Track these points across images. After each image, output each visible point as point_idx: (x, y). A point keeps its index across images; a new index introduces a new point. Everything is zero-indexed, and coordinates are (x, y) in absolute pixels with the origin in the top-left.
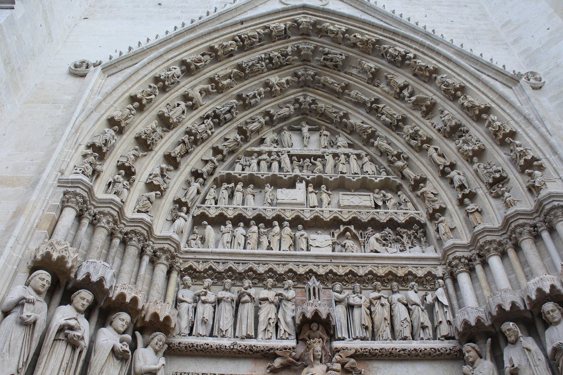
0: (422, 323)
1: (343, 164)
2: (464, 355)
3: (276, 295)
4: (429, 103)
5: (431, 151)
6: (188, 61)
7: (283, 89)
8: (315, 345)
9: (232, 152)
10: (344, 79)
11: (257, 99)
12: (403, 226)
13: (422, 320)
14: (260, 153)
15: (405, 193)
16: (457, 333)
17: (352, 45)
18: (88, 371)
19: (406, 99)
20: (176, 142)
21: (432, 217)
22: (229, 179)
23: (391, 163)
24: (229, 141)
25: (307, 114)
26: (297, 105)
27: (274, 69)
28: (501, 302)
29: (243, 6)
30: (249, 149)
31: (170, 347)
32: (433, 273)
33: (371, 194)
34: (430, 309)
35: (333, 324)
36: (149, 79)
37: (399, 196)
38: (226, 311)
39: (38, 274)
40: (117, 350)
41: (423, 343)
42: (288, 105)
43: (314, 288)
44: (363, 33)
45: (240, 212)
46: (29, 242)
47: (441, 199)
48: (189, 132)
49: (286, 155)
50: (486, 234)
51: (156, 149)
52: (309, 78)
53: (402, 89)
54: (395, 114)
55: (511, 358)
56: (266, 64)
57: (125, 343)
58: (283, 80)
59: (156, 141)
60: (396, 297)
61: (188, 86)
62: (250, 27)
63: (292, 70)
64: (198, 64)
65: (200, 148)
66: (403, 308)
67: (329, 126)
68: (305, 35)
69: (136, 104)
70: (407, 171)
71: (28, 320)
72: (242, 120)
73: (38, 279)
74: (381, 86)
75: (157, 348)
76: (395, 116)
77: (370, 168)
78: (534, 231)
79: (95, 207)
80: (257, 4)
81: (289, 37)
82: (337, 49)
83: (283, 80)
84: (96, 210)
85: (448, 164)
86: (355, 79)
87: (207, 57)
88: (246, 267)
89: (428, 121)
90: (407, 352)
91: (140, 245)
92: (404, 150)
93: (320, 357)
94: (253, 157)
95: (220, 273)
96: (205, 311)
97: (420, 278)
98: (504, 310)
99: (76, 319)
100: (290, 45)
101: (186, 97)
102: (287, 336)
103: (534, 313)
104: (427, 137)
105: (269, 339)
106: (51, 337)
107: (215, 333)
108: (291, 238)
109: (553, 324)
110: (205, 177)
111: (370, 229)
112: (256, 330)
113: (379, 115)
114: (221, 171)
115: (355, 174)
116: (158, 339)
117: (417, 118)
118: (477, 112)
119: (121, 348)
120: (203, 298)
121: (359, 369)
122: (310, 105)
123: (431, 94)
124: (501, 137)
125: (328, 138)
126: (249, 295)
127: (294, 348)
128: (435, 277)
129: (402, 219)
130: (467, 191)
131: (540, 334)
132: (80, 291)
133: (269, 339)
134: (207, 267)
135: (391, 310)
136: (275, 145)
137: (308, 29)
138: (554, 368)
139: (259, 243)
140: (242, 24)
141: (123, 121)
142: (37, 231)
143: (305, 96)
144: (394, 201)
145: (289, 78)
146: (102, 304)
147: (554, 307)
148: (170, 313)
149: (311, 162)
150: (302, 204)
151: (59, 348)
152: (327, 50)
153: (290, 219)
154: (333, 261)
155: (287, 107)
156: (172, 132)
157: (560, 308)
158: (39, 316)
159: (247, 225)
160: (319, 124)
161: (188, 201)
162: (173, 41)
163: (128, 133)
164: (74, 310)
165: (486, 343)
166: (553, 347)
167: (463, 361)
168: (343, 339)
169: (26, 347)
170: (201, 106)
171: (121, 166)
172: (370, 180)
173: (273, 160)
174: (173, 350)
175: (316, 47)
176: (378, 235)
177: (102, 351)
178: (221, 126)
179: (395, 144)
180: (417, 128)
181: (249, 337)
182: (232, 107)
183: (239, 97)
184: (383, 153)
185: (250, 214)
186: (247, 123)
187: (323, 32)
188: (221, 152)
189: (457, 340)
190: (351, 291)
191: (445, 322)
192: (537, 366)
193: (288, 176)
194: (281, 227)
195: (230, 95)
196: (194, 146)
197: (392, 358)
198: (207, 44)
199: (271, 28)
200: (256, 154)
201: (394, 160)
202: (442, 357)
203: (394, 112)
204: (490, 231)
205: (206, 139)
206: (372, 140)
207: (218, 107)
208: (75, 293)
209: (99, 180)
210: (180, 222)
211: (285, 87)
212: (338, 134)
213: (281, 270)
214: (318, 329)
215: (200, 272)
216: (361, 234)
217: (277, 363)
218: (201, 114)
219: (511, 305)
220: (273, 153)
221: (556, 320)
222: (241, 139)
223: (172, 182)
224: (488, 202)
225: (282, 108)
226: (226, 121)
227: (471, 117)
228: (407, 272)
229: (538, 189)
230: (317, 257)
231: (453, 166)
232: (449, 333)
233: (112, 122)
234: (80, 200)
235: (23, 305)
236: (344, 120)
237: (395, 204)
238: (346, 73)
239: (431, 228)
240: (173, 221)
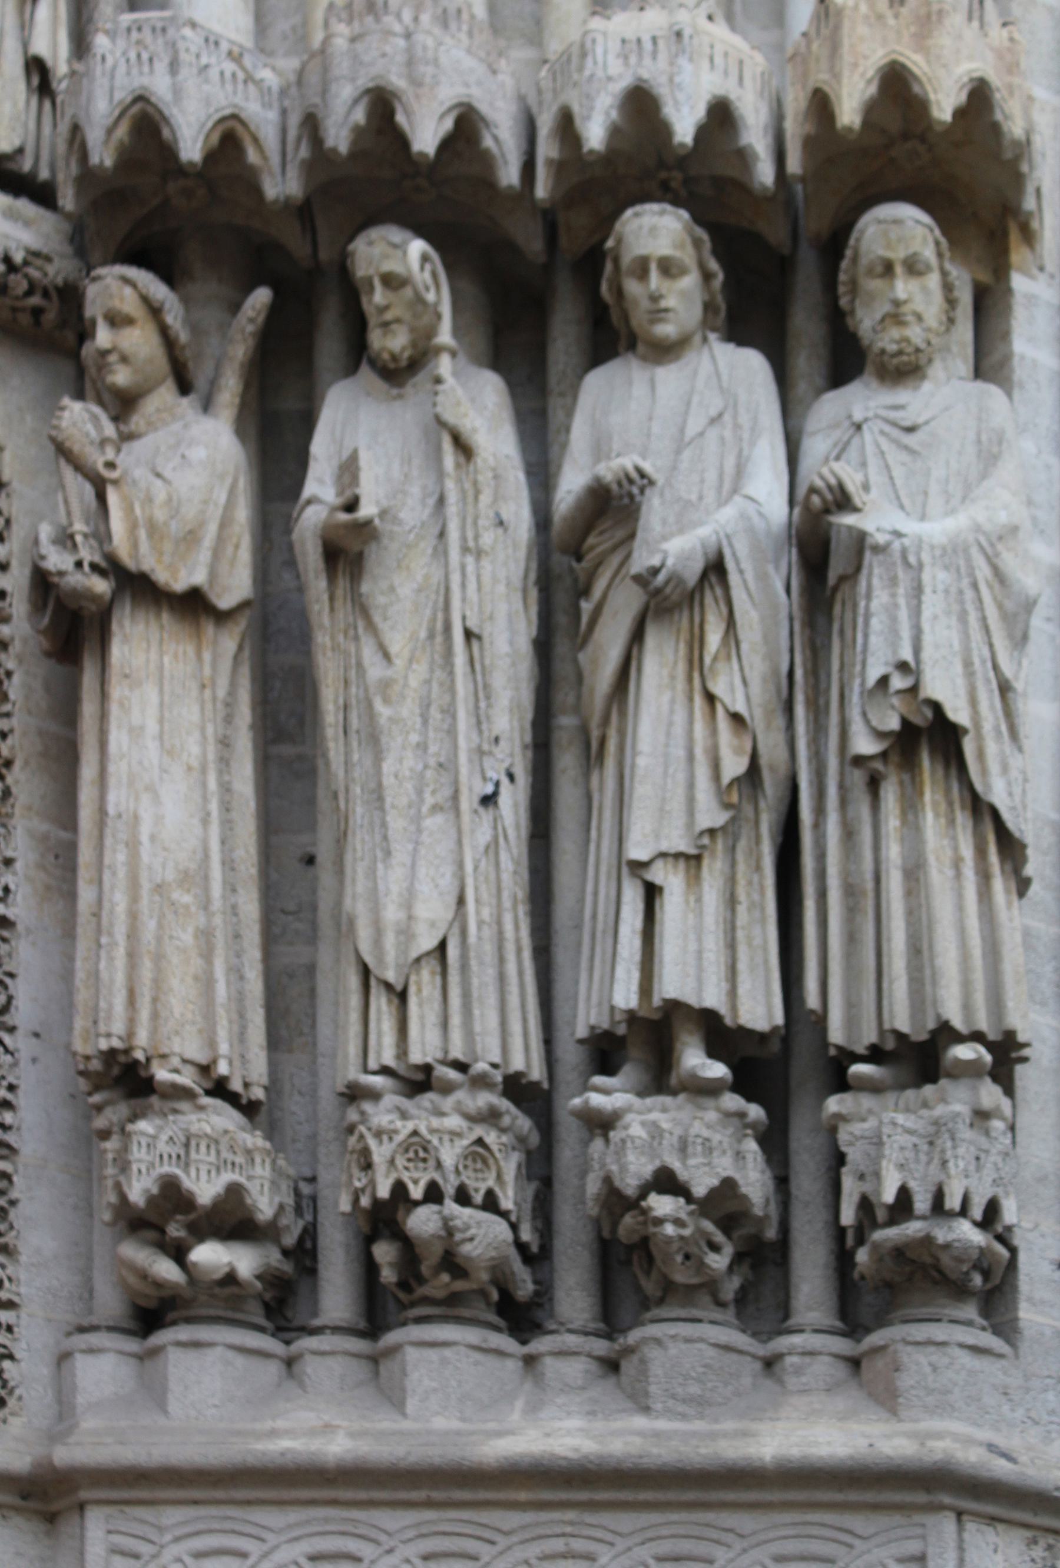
16: (74, 169)
28: (397, 81)
55: (354, 458)
98: (402, 141)
103: (563, 241)
109: (641, 348)
131: (553, 379)
138: (561, 598)
147: (681, 246)
157: (714, 265)
165: (235, 307)
166: (598, 480)
167: (68, 369)
189: (68, 216)
192: (479, 554)
219: (449, 124)
221: (667, 330)
232: (20, 151)
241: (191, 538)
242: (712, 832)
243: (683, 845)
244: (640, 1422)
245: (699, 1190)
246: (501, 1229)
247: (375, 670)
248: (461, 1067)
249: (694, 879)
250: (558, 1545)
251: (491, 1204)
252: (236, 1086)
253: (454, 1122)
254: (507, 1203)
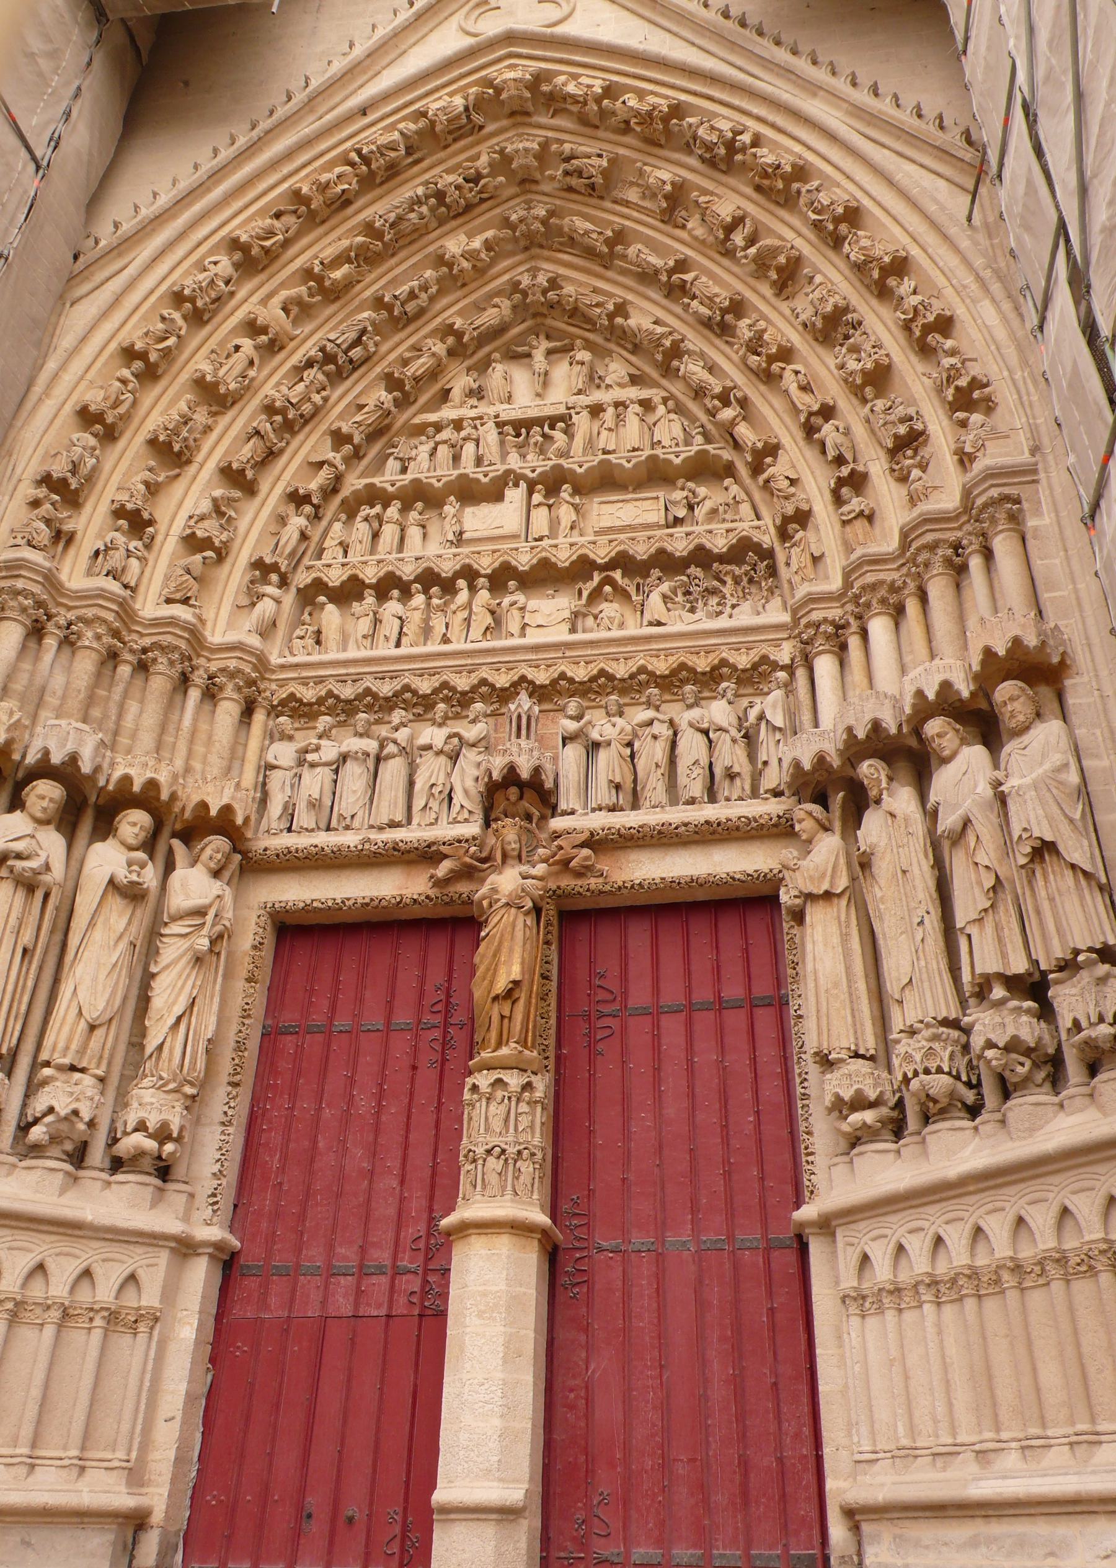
0: (728, 769)
1: (610, 430)
2: (792, 826)
3: (450, 737)
4: (782, 259)
5: (788, 375)
6: (244, 238)
7: (479, 264)
8: (505, 831)
9: (376, 433)
10: (615, 219)
11: (419, 301)
12: (722, 559)
13: (728, 763)
14: (438, 427)
15: (737, 481)
17: (623, 126)
19: (739, 254)
20: (244, 436)
21: (784, 535)
22: (374, 496)
23: (712, 413)
24: (366, 409)
25: (544, 316)
26: (518, 296)
27: (455, 217)
29: (369, 61)
30: (417, 420)
32: (772, 658)
33: (661, 494)
34: (750, 739)
35: (549, 784)
36: (161, 297)
37: (726, 489)
38: (354, 777)
41: (726, 807)
42: (496, 300)
43: (519, 717)
44: (644, 90)
45: (390, 568)
47: (804, 490)
48: (270, 409)
49: (491, 424)
50: (866, 568)
51: (199, 458)
52: (537, 226)
53: (730, 229)
54: (717, 295)
56: (432, 210)
58: (477, 243)
59: (195, 440)
60: (695, 714)
61: (255, 299)
62: (382, 119)
63: (498, 211)
64: (267, 243)
65: (301, 437)
66: (700, 738)
67: (591, 336)
68: (519, 114)
69: (138, 365)
70: (743, 430)
72: (392, 356)
74: (690, 225)
75: (212, 865)
76: (718, 300)
77: (669, 430)
78: (958, 555)
79: (69, 608)
80: (403, 47)
81: (481, 128)
82: (592, 142)
83: (477, 243)
84: (71, 615)
85: (816, 407)
86: (635, 214)
87: (290, 220)
88: (397, 685)
89: (786, 303)
90: (691, 828)
91: (175, 673)
92: (738, 378)
93: (516, 853)
94: (424, 438)
95: (348, 702)
96: (315, 782)
97: (744, 671)
100: (484, 148)
101: (253, 328)
102: (466, 815)
104: (780, 346)
105: (432, 824)
107: (334, 824)
108: (493, 613)
110: (315, 501)
111: (656, 573)
112: (409, 808)
113: (686, 300)
114: (354, 483)
115: (634, 450)
117: (764, 297)
118: (876, 274)
120: (310, 757)
121: (598, 866)
122: (545, 292)
123: (789, 235)
124: (918, 333)
125: (585, 369)
126: (395, 742)
127: (474, 838)
128: (775, 666)
129: (720, 544)
130: (845, 471)
133: (432, 824)
134: (323, 693)
135: (674, 744)
136: (474, 401)
137: (521, 97)
139: (426, 631)
140: (365, 114)
141: (109, 412)
143: (534, 272)
144: (708, 505)
145: (490, 234)
148: (233, 798)
149: (544, 435)
150: (515, 537)
152: (567, 147)
153: (489, 571)
154: (568, 654)
155: (495, 306)
156: (231, 414)
159: (406, 594)
160: (573, 337)
161: (280, 560)
162: (209, 190)
163: (128, 435)
168: (573, 813)
170: (292, 339)
171: (119, 513)
172: (665, 460)
173: (464, 439)
175: (545, 145)
176: (665, 587)
178: (347, 377)
179: (721, 369)
180: (762, 324)
181: (393, 825)
182: (364, 332)
183: (378, 303)
184: (699, 392)
185: (408, 571)
186: (405, 362)
187: (556, 102)
188: (348, 439)
190: (603, 711)
191: (774, 763)
193: (491, 475)
194: (473, 589)
195: (356, 302)
196: (287, 436)
197: (665, 840)
198: (286, 185)
199: (430, 113)
200: (431, 430)
201: (714, 407)
202: (765, 831)
203: (717, 290)
204: (877, 561)
205: (313, 416)
206: (675, 363)
207: (332, 336)
209: (72, 551)
210: (266, 607)
211: (482, 260)
212: (609, 353)
213: (463, 683)
214: (521, 798)
215: (310, 704)
216: (638, 585)
217: (444, 868)
218: (295, 360)
220: (465, 424)
222: (395, 400)
223: (243, 525)
224: (887, 493)
225: (485, 309)
226: (355, 366)
227: (868, 287)
228: (716, 662)
229: (972, 458)
230: (537, 648)
231: (827, 412)
233: (87, 417)
234: (26, 602)
236: (619, 320)
237: (714, 511)
238: (615, 202)
239: (781, 557)
240: (254, 604)
241: (823, 876)
242: (986, 910)
243: (976, 916)
244: (1010, 1145)
245: (1001, 1045)
246: (945, 1079)
247: (879, 894)
248: (921, 1022)
249: (982, 928)
250: (990, 1206)
251: (940, 1070)
252: (862, 1052)
253: (924, 1043)
254: (946, 1069)
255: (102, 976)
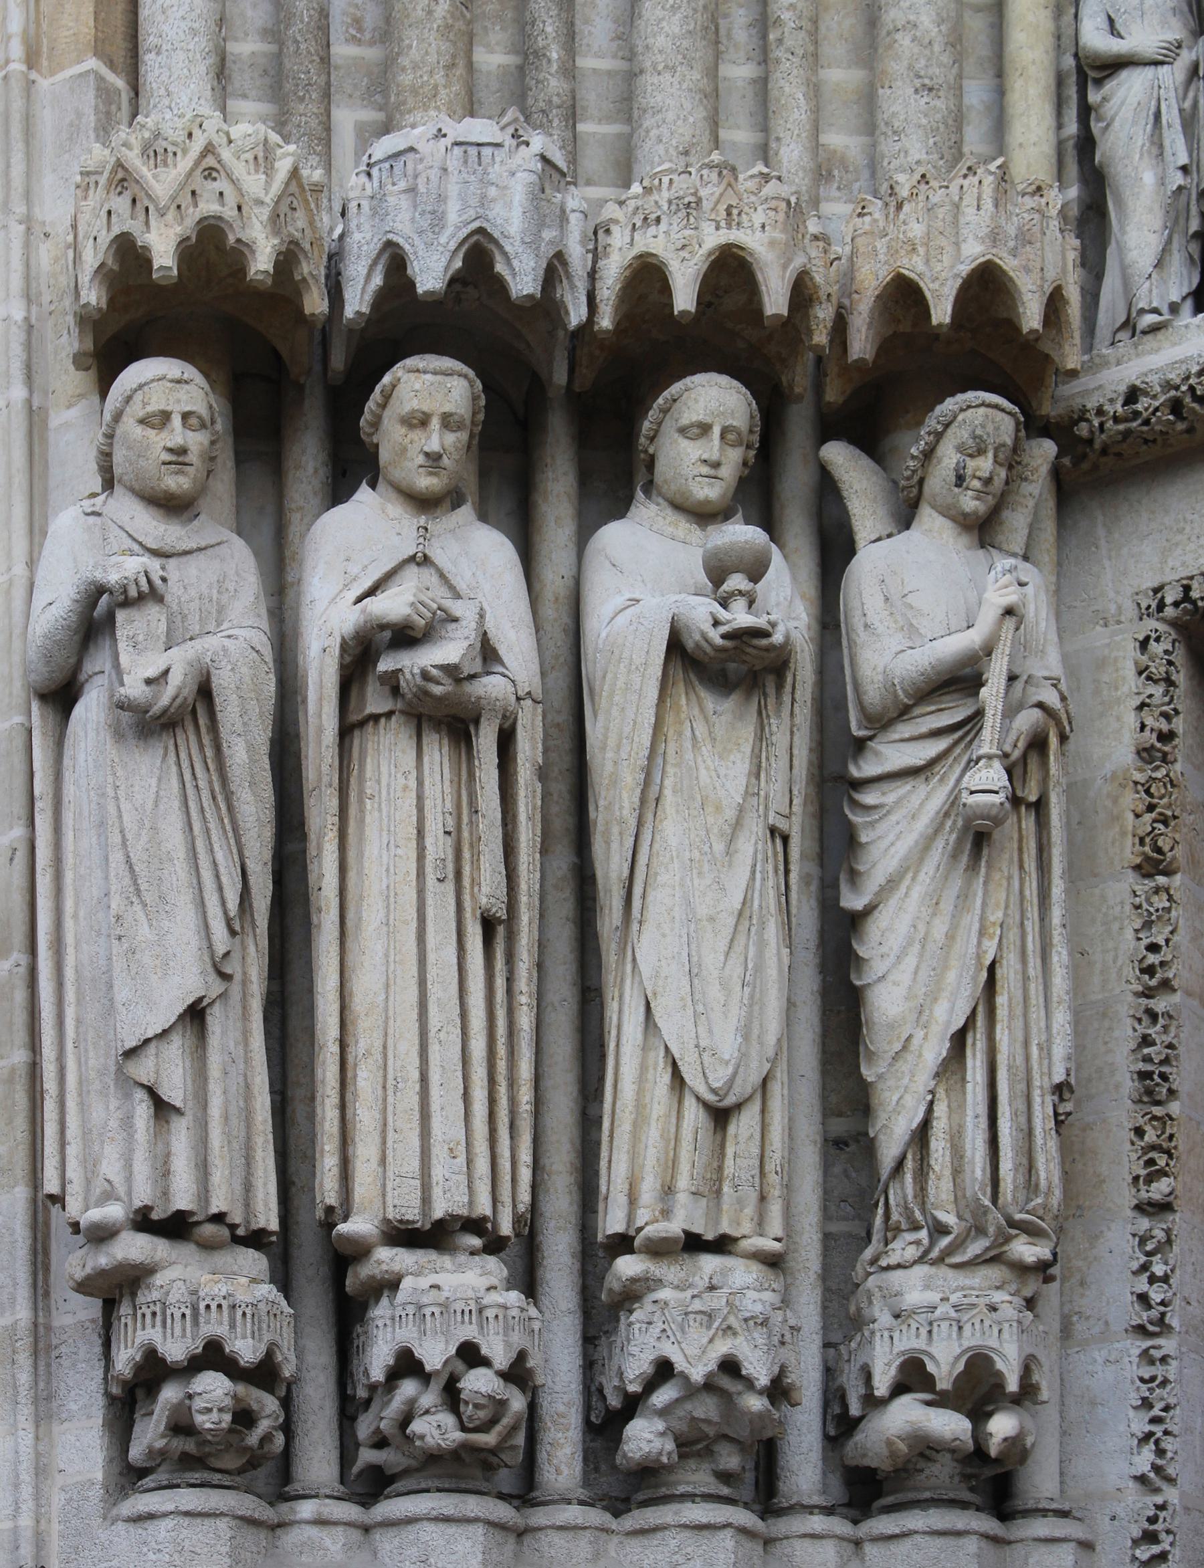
18: (592, 815)
31: (1080, 439)
39: (128, 399)
40: (697, 645)
46: (28, 196)
57: (737, 582)
71: (165, 701)
73: (139, 431)
75: (970, 503)
99: (425, 561)
106: (320, 730)
116: (960, 449)
119: (716, 623)
132: (387, 379)
142: (44, 84)
146: (560, 376)
151: (384, 769)
158: (212, 643)
164: (397, 510)
169: (213, 825)
174: (1104, 451)
177: (620, 684)
208: (371, 405)
235: (110, 619)
255: (712, 959)
